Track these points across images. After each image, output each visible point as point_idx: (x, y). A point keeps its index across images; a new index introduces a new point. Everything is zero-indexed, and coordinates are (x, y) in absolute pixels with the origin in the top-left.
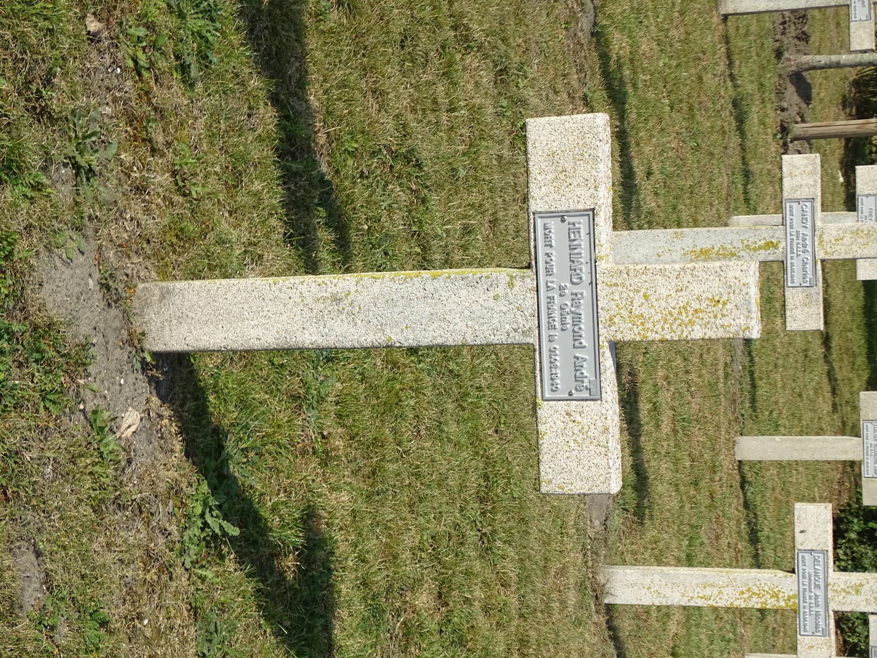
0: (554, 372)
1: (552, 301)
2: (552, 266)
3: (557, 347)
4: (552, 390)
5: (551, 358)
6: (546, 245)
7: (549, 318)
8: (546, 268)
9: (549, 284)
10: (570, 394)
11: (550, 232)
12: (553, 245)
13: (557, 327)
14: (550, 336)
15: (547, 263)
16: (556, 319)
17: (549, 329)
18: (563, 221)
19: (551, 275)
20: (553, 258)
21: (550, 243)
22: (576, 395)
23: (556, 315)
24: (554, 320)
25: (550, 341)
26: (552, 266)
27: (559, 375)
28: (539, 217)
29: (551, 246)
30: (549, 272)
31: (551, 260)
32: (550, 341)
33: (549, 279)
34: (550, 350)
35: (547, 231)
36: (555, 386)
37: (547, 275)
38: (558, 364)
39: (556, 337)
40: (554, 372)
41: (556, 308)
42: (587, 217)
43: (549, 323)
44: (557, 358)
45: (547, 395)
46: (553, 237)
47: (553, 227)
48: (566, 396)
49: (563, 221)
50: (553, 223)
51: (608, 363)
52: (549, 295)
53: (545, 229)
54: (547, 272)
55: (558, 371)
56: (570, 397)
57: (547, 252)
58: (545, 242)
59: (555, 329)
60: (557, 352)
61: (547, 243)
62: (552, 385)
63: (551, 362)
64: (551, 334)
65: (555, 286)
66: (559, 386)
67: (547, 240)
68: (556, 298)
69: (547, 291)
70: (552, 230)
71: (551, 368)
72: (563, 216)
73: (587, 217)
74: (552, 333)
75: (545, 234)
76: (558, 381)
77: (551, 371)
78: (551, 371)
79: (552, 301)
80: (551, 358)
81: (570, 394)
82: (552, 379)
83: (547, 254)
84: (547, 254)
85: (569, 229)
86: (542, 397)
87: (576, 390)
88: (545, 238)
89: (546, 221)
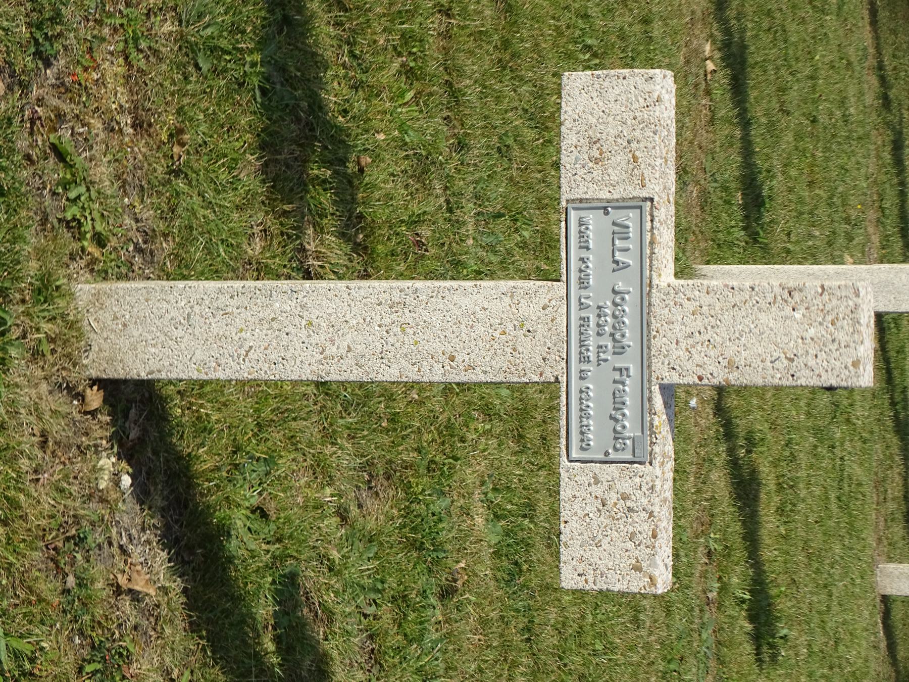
0: (585, 422)
1: (586, 324)
2: (589, 275)
3: (591, 386)
4: (582, 449)
5: (581, 403)
6: (581, 247)
7: (581, 346)
8: (580, 278)
9: (583, 300)
10: (607, 454)
11: (587, 229)
12: (591, 246)
13: (591, 359)
14: (581, 371)
15: (581, 271)
16: (591, 348)
17: (580, 361)
18: (607, 213)
19: (586, 288)
20: (590, 265)
21: (586, 244)
22: (613, 456)
23: (592, 343)
24: (588, 350)
25: (581, 378)
26: (589, 275)
27: (592, 428)
28: (574, 209)
29: (588, 248)
30: (583, 284)
31: (587, 267)
32: (581, 378)
33: (584, 293)
34: (581, 392)
35: (584, 227)
36: (587, 442)
37: (580, 288)
38: (591, 412)
39: (589, 374)
40: (585, 422)
41: (591, 333)
42: (639, 211)
43: (581, 353)
44: (591, 405)
45: (574, 455)
46: (591, 236)
47: (591, 222)
48: (601, 457)
49: (607, 213)
50: (591, 217)
51: (661, 420)
52: (583, 315)
53: (581, 225)
54: (581, 283)
55: (591, 422)
56: (607, 459)
57: (582, 256)
58: (580, 242)
59: (589, 361)
60: (591, 394)
61: (582, 244)
62: (582, 441)
63: (581, 410)
64: (583, 368)
65: (591, 304)
66: (591, 443)
67: (582, 240)
68: (591, 319)
69: (580, 309)
70: (590, 227)
71: (581, 417)
72: (605, 208)
73: (639, 211)
74: (584, 367)
75: (580, 232)
76: (591, 436)
77: (581, 422)
78: (581, 422)
79: (586, 324)
80: (581, 403)
81: (606, 455)
82: (582, 433)
83: (582, 260)
84: (582, 260)
85: (614, 233)
86: (568, 456)
87: (616, 449)
88: (580, 237)
89: (583, 213)
